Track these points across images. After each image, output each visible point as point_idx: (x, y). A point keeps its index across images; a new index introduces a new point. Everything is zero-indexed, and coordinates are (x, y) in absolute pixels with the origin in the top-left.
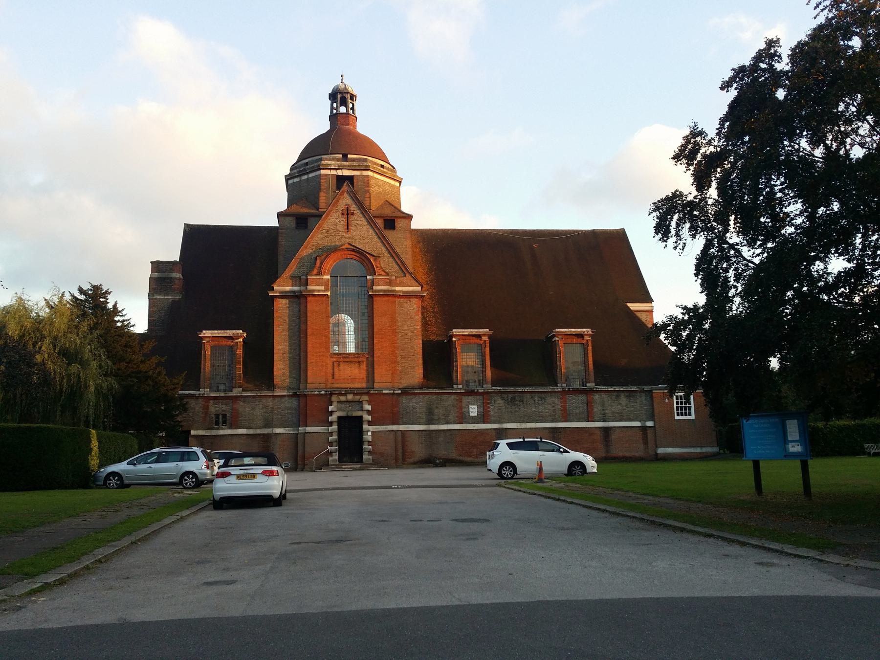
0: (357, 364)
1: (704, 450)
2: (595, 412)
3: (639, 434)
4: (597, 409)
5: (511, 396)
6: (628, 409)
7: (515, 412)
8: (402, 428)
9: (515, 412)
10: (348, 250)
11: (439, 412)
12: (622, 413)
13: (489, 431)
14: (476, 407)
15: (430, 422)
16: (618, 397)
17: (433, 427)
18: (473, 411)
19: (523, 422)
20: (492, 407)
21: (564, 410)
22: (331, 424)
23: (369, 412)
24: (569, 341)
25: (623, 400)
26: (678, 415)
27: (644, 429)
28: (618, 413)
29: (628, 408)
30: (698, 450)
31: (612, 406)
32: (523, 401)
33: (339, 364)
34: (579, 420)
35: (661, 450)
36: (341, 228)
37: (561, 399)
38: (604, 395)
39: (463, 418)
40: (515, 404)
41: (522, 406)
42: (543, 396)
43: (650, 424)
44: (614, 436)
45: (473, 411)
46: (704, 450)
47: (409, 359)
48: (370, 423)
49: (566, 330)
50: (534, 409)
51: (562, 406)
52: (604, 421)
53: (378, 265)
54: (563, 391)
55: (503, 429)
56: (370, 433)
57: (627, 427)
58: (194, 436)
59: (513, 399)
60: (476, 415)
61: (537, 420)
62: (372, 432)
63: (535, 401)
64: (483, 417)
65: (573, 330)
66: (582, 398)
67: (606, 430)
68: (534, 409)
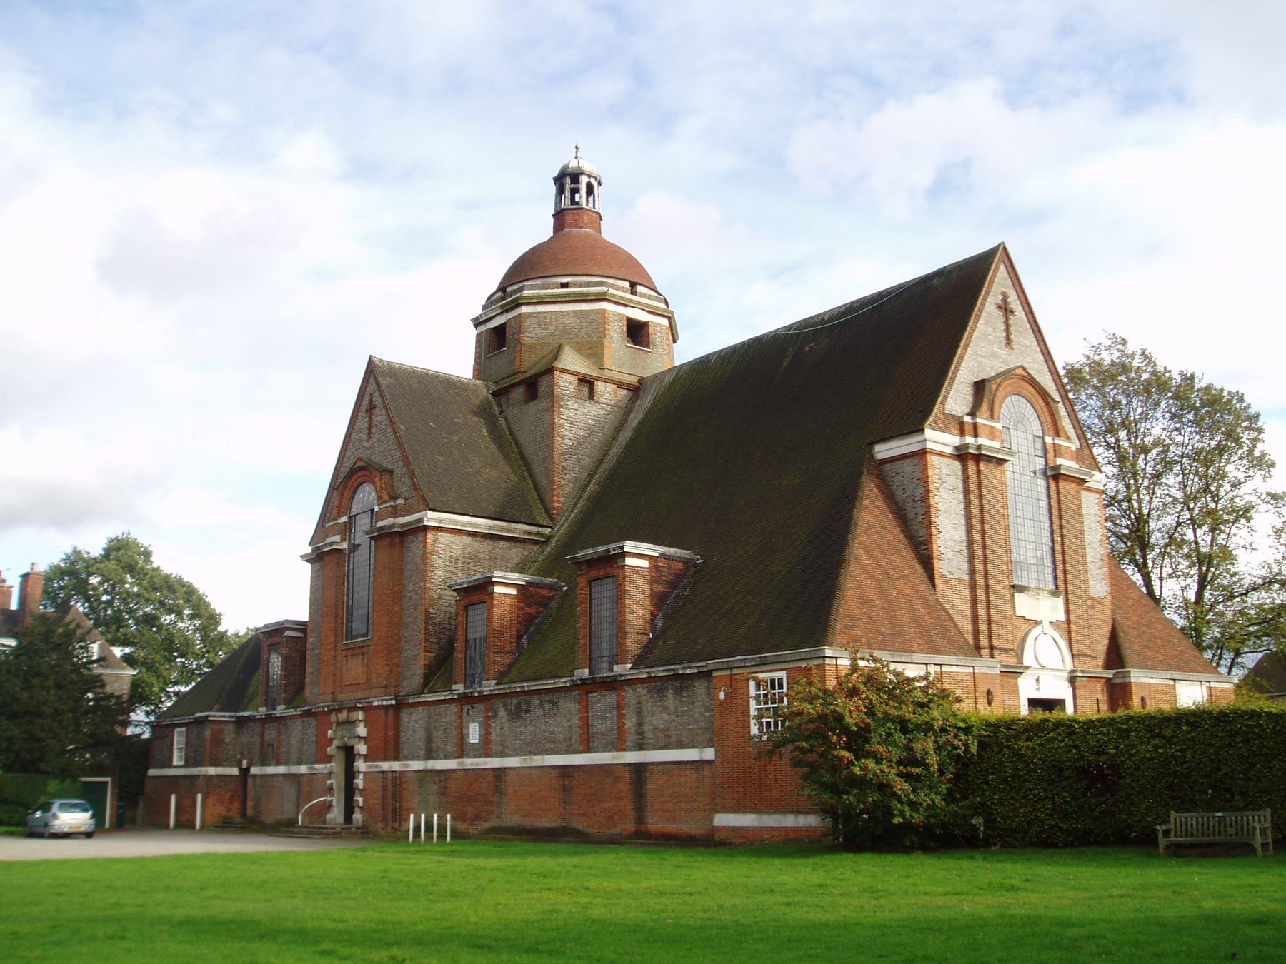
0: (361, 657)
2: (627, 729)
4: (630, 722)
5: (515, 701)
6: (679, 720)
7: (521, 733)
9: (521, 733)
11: (438, 736)
12: (668, 730)
13: (486, 773)
14: (477, 725)
15: (429, 756)
16: (662, 692)
18: (474, 734)
19: (531, 753)
21: (586, 726)
22: (328, 759)
23: (365, 740)
24: (593, 574)
25: (671, 700)
28: (663, 730)
29: (678, 716)
30: (790, 821)
31: (653, 714)
32: (529, 711)
33: (347, 660)
34: (606, 748)
35: (724, 820)
36: (364, 437)
37: (579, 702)
39: (462, 749)
40: (520, 718)
41: (528, 722)
42: (555, 697)
44: (651, 783)
45: (474, 734)
46: (790, 821)
47: (412, 643)
48: (366, 758)
49: (590, 551)
50: (543, 728)
51: (581, 719)
52: (640, 747)
54: (649, 677)
55: (506, 768)
56: (361, 776)
57: (680, 763)
58: (254, 776)
59: (518, 706)
60: (477, 741)
61: (547, 750)
62: (365, 773)
64: (485, 748)
65: (600, 549)
66: (611, 697)
67: (639, 770)
68: (543, 728)
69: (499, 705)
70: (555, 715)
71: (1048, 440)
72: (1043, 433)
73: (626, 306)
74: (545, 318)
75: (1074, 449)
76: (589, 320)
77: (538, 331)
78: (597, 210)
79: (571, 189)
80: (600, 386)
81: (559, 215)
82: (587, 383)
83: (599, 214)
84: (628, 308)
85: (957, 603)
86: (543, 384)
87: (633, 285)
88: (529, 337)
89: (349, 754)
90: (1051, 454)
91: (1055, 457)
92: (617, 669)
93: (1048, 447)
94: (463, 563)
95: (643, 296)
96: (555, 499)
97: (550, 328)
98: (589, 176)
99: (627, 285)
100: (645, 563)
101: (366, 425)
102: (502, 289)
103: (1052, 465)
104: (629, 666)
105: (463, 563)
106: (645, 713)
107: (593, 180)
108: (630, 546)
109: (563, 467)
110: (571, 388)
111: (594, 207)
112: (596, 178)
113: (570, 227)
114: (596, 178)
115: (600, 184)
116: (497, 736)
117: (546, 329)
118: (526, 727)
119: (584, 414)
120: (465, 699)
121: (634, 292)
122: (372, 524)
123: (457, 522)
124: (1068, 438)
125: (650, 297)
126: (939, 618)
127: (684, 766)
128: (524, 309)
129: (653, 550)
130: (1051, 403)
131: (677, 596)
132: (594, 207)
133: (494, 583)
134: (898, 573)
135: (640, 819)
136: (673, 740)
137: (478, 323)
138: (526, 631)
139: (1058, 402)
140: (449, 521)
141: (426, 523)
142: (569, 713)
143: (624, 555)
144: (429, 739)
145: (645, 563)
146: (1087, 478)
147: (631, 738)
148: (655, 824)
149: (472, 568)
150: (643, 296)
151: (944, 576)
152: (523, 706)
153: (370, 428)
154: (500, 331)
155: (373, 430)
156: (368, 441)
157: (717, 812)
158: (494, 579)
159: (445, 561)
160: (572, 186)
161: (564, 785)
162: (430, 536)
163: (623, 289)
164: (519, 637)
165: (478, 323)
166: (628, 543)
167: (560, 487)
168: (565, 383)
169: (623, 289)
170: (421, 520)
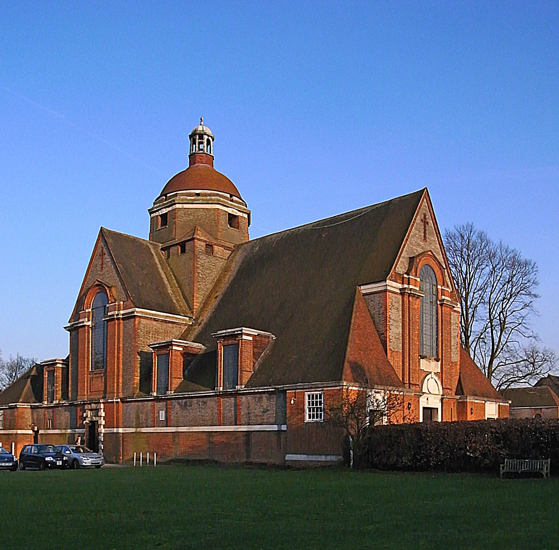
1: (329, 458)
3: (274, 438)
7: (187, 416)
8: (121, 430)
9: (187, 416)
10: (97, 285)
11: (142, 417)
17: (138, 430)
18: (162, 416)
20: (172, 412)
26: (310, 418)
27: (279, 432)
38: (249, 397)
40: (187, 409)
43: (284, 428)
50: (199, 414)
53: (111, 294)
62: (104, 433)
63: (199, 405)
69: (175, 402)
70: (205, 408)
71: (439, 287)
72: (437, 283)
73: (228, 207)
74: (188, 211)
75: (450, 292)
76: (210, 214)
77: (184, 218)
78: (212, 155)
79: (199, 142)
80: (216, 247)
81: (192, 157)
82: (210, 246)
83: (213, 157)
84: (229, 208)
85: (396, 362)
86: (188, 246)
87: (231, 196)
88: (180, 220)
89: (94, 425)
90: (440, 294)
91: (442, 295)
92: (238, 387)
93: (439, 290)
94: (152, 334)
95: (236, 202)
96: (195, 304)
97: (191, 217)
98: (208, 136)
99: (228, 196)
100: (251, 338)
101: (100, 263)
102: (164, 194)
103: (440, 299)
104: (243, 386)
105: (152, 334)
106: (251, 408)
107: (210, 138)
108: (245, 330)
109: (198, 288)
110: (203, 248)
111: (207, 152)
112: (211, 137)
113: (198, 162)
114: (211, 137)
115: (213, 141)
116: (174, 417)
117: (188, 217)
118: (189, 413)
119: (208, 262)
120: (157, 399)
121: (232, 201)
122: (104, 313)
123: (150, 314)
124: (448, 286)
125: (239, 203)
126: (389, 369)
127: (270, 433)
128: (178, 206)
129: (255, 332)
130: (442, 269)
131: (265, 354)
132: (210, 153)
133: (172, 345)
134: (371, 347)
135: (248, 457)
136: (265, 421)
137: (151, 212)
138: (187, 368)
139: (444, 269)
140: (147, 313)
141: (135, 314)
142: (212, 407)
143: (242, 334)
144: (138, 417)
145: (251, 338)
146: (455, 306)
147: (244, 420)
148: (255, 459)
149: (156, 337)
150: (236, 202)
151: (390, 350)
152: (188, 404)
153: (102, 264)
154: (164, 217)
155: (104, 266)
156: (101, 271)
157: (287, 454)
158: (173, 343)
159: (144, 333)
160: (200, 141)
161: (209, 440)
162: (137, 319)
163: (227, 198)
164: (184, 371)
165: (151, 212)
166: (243, 328)
167: (197, 298)
168: (200, 246)
169: (227, 198)
170: (133, 312)
